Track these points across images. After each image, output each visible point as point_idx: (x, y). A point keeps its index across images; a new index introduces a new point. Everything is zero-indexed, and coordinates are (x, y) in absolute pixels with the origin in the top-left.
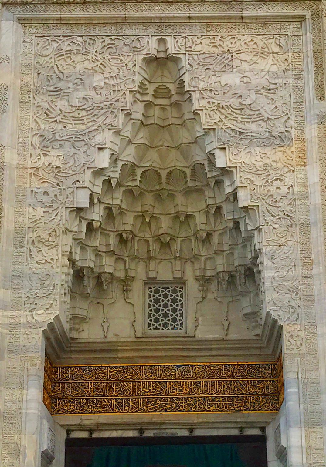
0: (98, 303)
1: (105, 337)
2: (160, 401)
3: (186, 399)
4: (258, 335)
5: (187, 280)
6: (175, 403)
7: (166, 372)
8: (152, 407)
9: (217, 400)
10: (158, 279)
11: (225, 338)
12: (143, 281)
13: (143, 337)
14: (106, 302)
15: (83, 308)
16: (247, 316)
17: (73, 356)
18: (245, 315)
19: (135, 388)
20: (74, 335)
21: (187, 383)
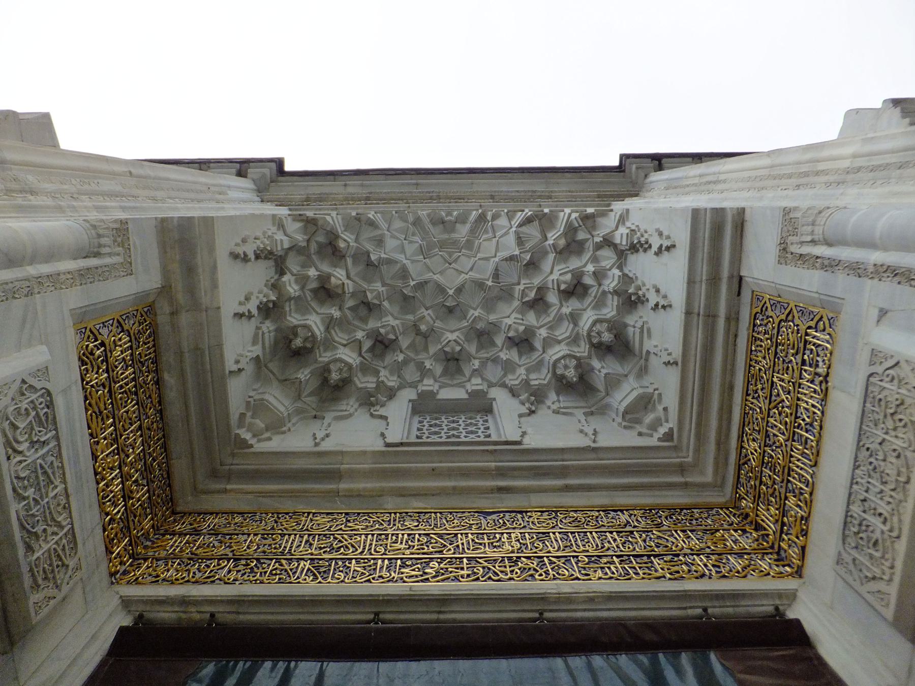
0: (315, 417)
1: (316, 445)
2: (439, 563)
3: (514, 561)
4: (669, 436)
5: (494, 399)
6: (484, 568)
7: (455, 521)
8: (413, 573)
9: (604, 560)
10: (439, 397)
11: (593, 445)
12: (410, 401)
13: (402, 444)
14: (329, 416)
15: (278, 400)
16: (628, 417)
17: (229, 487)
18: (626, 413)
19: (371, 544)
20: (246, 435)
21: (513, 535)
